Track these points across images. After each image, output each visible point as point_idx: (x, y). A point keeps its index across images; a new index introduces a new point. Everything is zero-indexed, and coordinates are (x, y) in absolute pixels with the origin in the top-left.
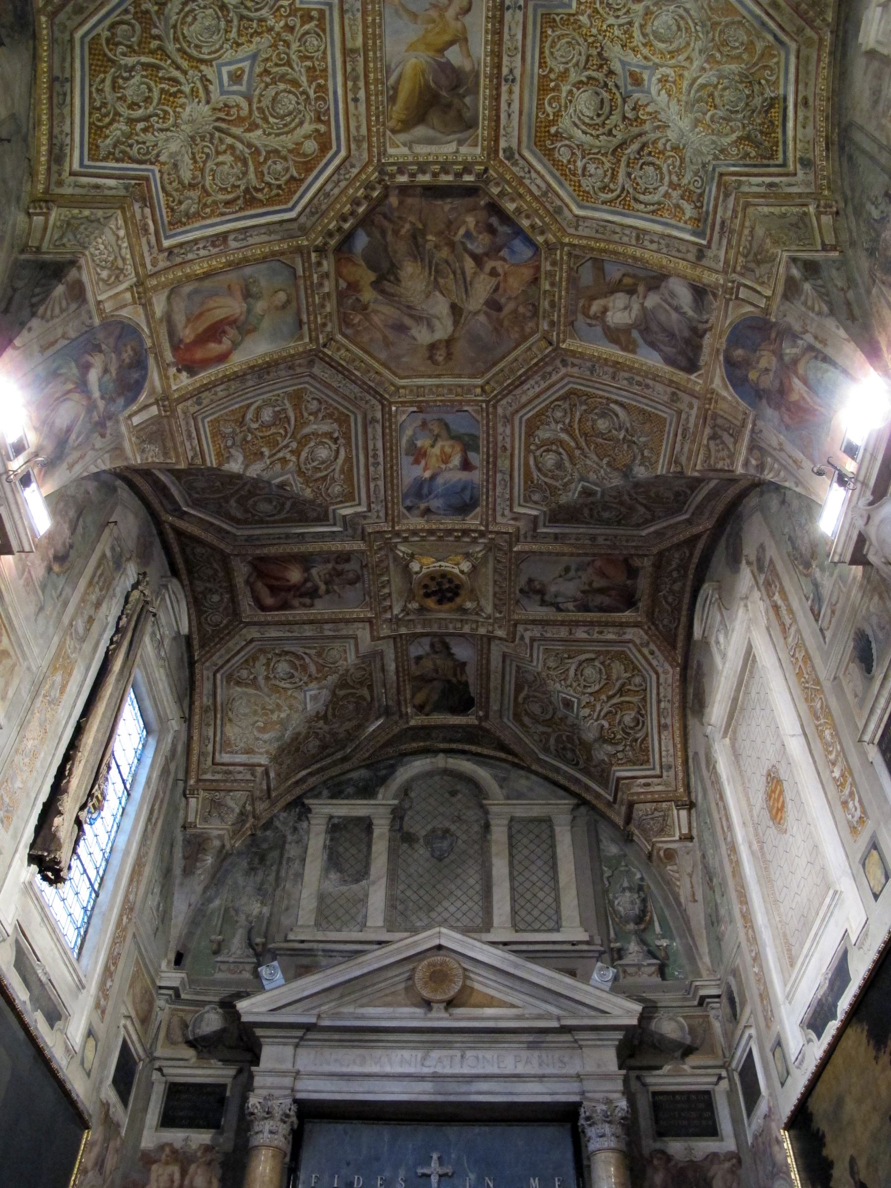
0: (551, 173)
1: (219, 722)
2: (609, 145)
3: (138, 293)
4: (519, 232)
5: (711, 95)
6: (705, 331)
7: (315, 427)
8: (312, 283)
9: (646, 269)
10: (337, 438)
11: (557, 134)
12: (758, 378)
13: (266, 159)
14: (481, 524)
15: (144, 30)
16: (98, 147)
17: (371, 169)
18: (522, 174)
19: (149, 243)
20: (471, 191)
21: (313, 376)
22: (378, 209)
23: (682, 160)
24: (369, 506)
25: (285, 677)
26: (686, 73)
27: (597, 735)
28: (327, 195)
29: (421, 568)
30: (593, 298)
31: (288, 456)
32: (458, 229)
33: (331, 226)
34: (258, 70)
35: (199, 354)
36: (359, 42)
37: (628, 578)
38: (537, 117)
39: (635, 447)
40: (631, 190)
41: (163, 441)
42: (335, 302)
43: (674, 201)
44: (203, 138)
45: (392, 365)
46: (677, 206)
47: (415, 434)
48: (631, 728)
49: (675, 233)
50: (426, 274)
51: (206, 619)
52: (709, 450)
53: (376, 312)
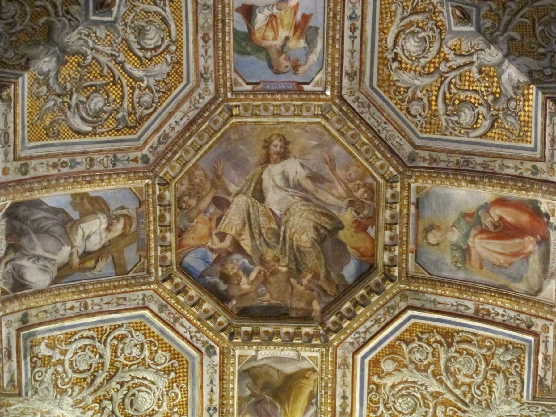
2: (122, 375)
6: (6, 254)
7: (417, 82)
8: (401, 247)
9: (73, 286)
10: (394, 60)
11: (170, 371)
13: (429, 364)
17: (335, 344)
18: (198, 335)
19: (546, 347)
21: (412, 144)
22: (331, 299)
23: (56, 386)
28: (377, 321)
30: (123, 235)
31: (451, 56)
32: (257, 277)
35: (524, 218)
38: (187, 384)
40: (98, 344)
42: (381, 218)
43: (57, 351)
44: (480, 403)
45: (327, 137)
47: (307, 56)
49: (52, 326)
50: (288, 234)
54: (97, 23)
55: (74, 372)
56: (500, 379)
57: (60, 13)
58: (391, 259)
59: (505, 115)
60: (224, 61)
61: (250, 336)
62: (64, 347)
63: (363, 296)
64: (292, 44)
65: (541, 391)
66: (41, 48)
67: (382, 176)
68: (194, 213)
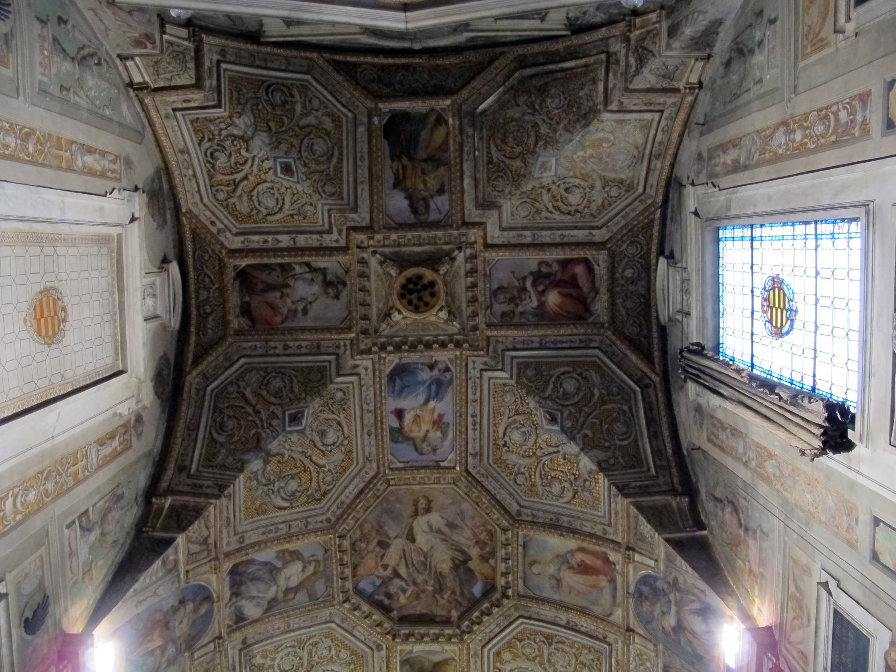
1: (649, 146)
6: (230, 600)
9: (280, 613)
10: (504, 445)
11: (350, 663)
13: (536, 656)
14: (385, 358)
20: (404, 620)
24: (481, 377)
25: (574, 189)
27: (251, 143)
28: (498, 625)
29: (437, 313)
30: (314, 574)
31: (544, 445)
32: (411, 595)
35: (599, 563)
37: (249, 304)
39: (264, 481)
41: (636, 528)
45: (458, 497)
47: (442, 442)
48: (218, 151)
51: (642, 247)
52: (207, 527)
53: (469, 539)
54: (291, 432)
57: (265, 426)
58: (507, 583)
59: (583, 490)
60: (383, 450)
61: (408, 636)
63: (487, 608)
64: (431, 435)
66: (252, 454)
67: (498, 525)
68: (365, 552)
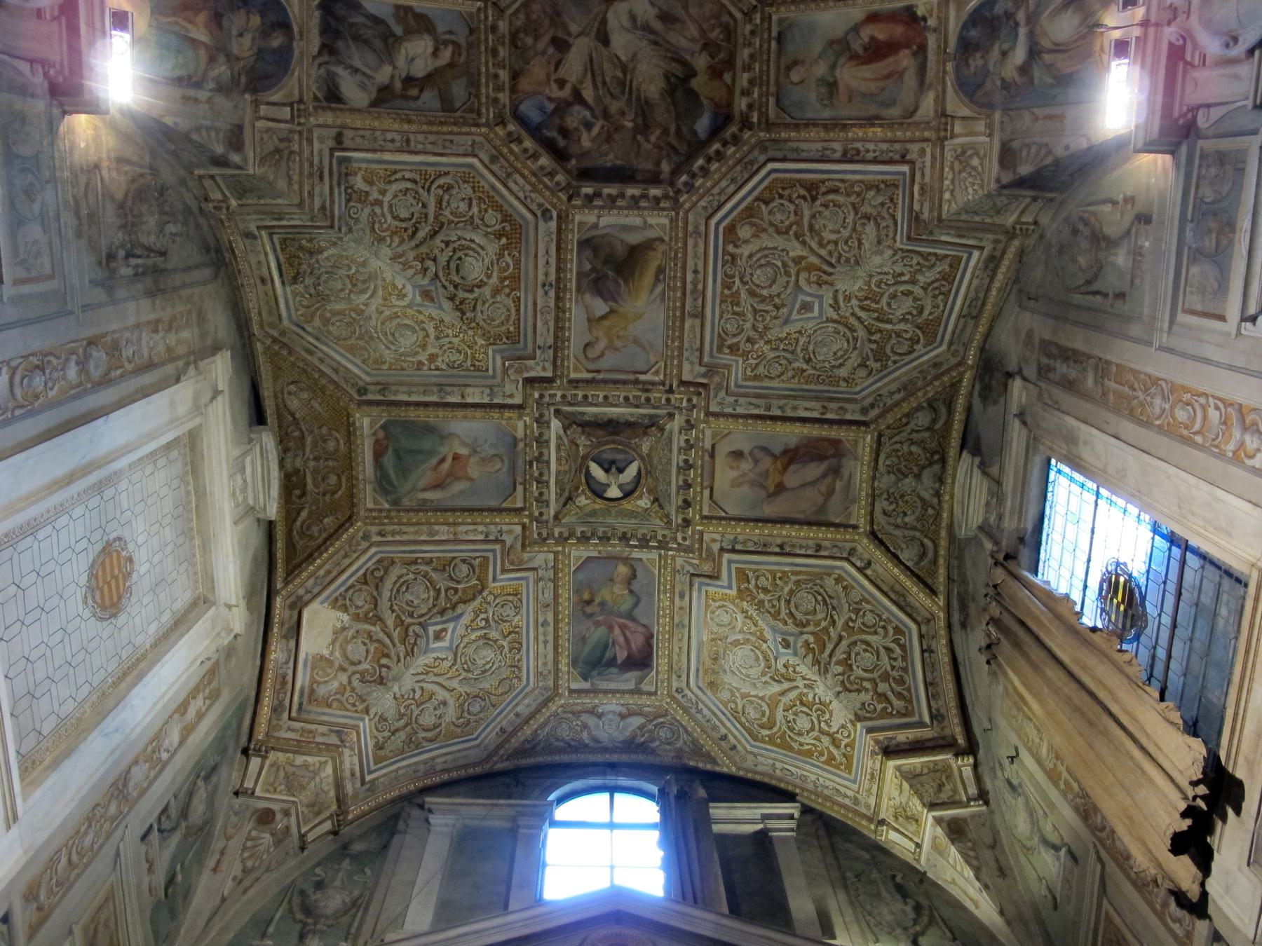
0: (502, 196)
3: (946, 130)
4: (535, 132)
5: (354, 285)
6: (320, 53)
8: (760, 87)
12: (249, 19)
13: (790, 226)
15: (883, 348)
16: (951, 266)
17: (687, 206)
18: (533, 195)
19: (923, 174)
20: (586, 174)
23: (373, 230)
26: (381, 301)
28: (733, 180)
30: (451, 65)
32: (599, 134)
33: (733, 149)
34: (785, 310)
36: (688, 324)
43: (375, 188)
44: (848, 260)
46: (371, 183)
49: (369, 156)
50: (634, 84)
53: (693, 40)
55: (394, 218)
56: (870, 229)
61: (590, 199)
62: (382, 186)
65: (917, 228)
68: (531, 53)
